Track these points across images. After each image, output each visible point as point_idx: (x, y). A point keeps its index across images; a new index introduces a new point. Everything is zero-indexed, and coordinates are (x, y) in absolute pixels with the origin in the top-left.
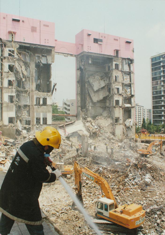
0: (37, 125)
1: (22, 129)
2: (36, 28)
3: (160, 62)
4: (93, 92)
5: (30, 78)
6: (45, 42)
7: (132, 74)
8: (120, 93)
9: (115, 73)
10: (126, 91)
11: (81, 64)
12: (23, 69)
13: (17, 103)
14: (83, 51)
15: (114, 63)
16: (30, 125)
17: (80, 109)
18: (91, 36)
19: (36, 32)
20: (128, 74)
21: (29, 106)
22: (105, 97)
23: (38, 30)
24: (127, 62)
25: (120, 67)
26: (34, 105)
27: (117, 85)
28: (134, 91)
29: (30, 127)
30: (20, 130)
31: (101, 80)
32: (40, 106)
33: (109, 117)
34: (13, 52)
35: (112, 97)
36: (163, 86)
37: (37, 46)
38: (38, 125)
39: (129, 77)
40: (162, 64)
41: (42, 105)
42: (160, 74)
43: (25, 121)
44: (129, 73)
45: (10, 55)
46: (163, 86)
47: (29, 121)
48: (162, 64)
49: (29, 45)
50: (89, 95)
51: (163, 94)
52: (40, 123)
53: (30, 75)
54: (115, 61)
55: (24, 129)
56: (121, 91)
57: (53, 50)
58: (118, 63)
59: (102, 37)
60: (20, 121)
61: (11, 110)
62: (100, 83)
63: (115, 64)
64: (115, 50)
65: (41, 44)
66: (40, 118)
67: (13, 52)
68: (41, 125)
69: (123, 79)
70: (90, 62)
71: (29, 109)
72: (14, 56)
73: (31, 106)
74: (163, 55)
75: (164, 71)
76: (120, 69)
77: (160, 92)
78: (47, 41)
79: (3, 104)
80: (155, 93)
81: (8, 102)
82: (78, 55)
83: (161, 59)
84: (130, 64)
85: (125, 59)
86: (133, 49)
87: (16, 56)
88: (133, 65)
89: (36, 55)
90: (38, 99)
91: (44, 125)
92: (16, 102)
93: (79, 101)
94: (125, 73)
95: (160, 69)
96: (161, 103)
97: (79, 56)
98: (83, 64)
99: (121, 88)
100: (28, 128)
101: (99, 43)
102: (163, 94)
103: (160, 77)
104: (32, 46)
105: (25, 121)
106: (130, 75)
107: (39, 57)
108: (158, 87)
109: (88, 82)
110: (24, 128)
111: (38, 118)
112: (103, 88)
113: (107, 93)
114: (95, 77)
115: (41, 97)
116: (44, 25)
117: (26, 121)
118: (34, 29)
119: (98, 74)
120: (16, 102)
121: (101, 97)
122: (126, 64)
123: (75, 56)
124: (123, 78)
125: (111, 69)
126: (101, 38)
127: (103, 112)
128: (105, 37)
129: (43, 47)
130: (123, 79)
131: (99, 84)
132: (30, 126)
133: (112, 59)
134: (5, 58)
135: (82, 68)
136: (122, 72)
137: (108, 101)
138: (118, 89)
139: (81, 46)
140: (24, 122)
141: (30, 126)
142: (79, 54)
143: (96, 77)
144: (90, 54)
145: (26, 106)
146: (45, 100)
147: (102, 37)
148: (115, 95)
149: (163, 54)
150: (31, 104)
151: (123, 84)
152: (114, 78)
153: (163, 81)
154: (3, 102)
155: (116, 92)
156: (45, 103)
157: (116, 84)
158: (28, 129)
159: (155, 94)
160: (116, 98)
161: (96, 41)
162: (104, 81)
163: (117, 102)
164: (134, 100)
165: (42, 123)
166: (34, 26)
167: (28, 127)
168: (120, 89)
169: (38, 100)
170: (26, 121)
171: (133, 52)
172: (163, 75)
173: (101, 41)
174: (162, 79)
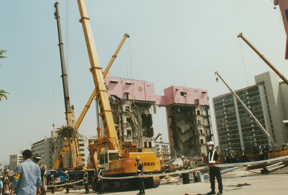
2: (142, 88)
3: (222, 103)
4: (181, 135)
6: (149, 98)
7: (209, 118)
8: (203, 134)
9: (199, 118)
10: (207, 132)
11: (172, 112)
14: (174, 103)
15: (196, 110)
17: (174, 148)
18: (178, 90)
19: (142, 91)
20: (206, 118)
22: (190, 138)
23: (143, 90)
24: (205, 108)
25: (201, 113)
27: (200, 127)
28: (212, 131)
31: (186, 124)
33: (196, 154)
34: (129, 108)
35: (198, 137)
36: (227, 123)
39: (207, 120)
40: (224, 104)
42: (223, 112)
44: (207, 117)
45: (126, 110)
46: (227, 123)
48: (224, 104)
49: (138, 102)
50: (179, 137)
51: (228, 130)
54: (197, 108)
56: (204, 132)
57: (154, 104)
58: (199, 110)
59: (186, 90)
62: (185, 126)
63: (197, 111)
64: (195, 100)
65: (147, 100)
67: (129, 108)
69: (204, 122)
70: (179, 110)
72: (129, 111)
74: (225, 96)
75: (226, 110)
76: (201, 115)
77: (226, 129)
78: (150, 98)
80: (220, 130)
82: (168, 106)
83: (223, 100)
84: (207, 109)
85: (203, 106)
86: (208, 97)
87: (131, 111)
88: (209, 110)
89: (142, 108)
90: (145, 143)
93: (172, 142)
94: (204, 118)
95: (223, 109)
96: (227, 139)
97: (169, 106)
98: (173, 112)
99: (203, 129)
101: (185, 95)
102: (228, 130)
103: (224, 115)
104: (141, 102)
106: (208, 118)
107: (143, 110)
108: (223, 125)
109: (178, 127)
112: (188, 130)
113: (192, 134)
114: (181, 122)
116: (147, 86)
118: (140, 90)
119: (183, 119)
121: (188, 138)
122: (204, 110)
123: (166, 106)
124: (204, 121)
125: (193, 115)
126: (185, 92)
127: (189, 150)
128: (188, 90)
129: (148, 102)
130: (204, 122)
131: (185, 128)
133: (194, 107)
134: (123, 113)
135: (173, 115)
136: (202, 116)
137: (193, 141)
138: (201, 130)
139: (171, 98)
142: (170, 105)
143: (182, 122)
144: (179, 105)
147: (186, 90)
148: (200, 136)
149: (224, 96)
151: (204, 126)
152: (198, 122)
153: (227, 119)
155: (200, 134)
156: (150, 146)
157: (200, 126)
159: (220, 131)
160: (201, 138)
161: (182, 94)
162: (189, 124)
163: (202, 140)
164: (213, 138)
166: (141, 87)
168: (203, 131)
169: (145, 143)
171: (208, 99)
172: (226, 114)
173: (186, 94)
174: (226, 117)
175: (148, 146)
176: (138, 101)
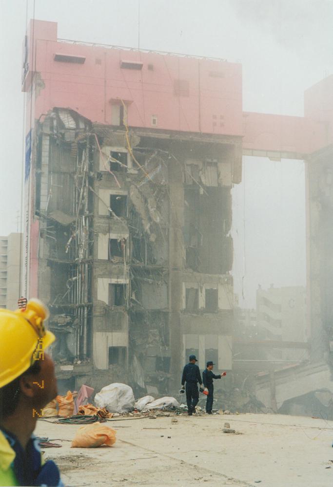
1: (146, 383)
5: (168, 229)
12: (150, 207)
13: (133, 306)
29: (168, 378)
30: (139, 386)
37: (191, 137)
53: (169, 221)
60: (141, 358)
61: (116, 327)
73: (170, 315)
79: (94, 308)
81: (107, 304)
92: (132, 304)
100: (162, 379)
110: (150, 380)
111: (191, 349)
115: (201, 288)
117: (158, 359)
120: (129, 305)
141: (169, 376)
145: (157, 313)
146: (212, 297)
150: (170, 309)
158: (161, 382)
167: (161, 378)
170: (158, 359)
175: (202, 304)
176: (165, 131)
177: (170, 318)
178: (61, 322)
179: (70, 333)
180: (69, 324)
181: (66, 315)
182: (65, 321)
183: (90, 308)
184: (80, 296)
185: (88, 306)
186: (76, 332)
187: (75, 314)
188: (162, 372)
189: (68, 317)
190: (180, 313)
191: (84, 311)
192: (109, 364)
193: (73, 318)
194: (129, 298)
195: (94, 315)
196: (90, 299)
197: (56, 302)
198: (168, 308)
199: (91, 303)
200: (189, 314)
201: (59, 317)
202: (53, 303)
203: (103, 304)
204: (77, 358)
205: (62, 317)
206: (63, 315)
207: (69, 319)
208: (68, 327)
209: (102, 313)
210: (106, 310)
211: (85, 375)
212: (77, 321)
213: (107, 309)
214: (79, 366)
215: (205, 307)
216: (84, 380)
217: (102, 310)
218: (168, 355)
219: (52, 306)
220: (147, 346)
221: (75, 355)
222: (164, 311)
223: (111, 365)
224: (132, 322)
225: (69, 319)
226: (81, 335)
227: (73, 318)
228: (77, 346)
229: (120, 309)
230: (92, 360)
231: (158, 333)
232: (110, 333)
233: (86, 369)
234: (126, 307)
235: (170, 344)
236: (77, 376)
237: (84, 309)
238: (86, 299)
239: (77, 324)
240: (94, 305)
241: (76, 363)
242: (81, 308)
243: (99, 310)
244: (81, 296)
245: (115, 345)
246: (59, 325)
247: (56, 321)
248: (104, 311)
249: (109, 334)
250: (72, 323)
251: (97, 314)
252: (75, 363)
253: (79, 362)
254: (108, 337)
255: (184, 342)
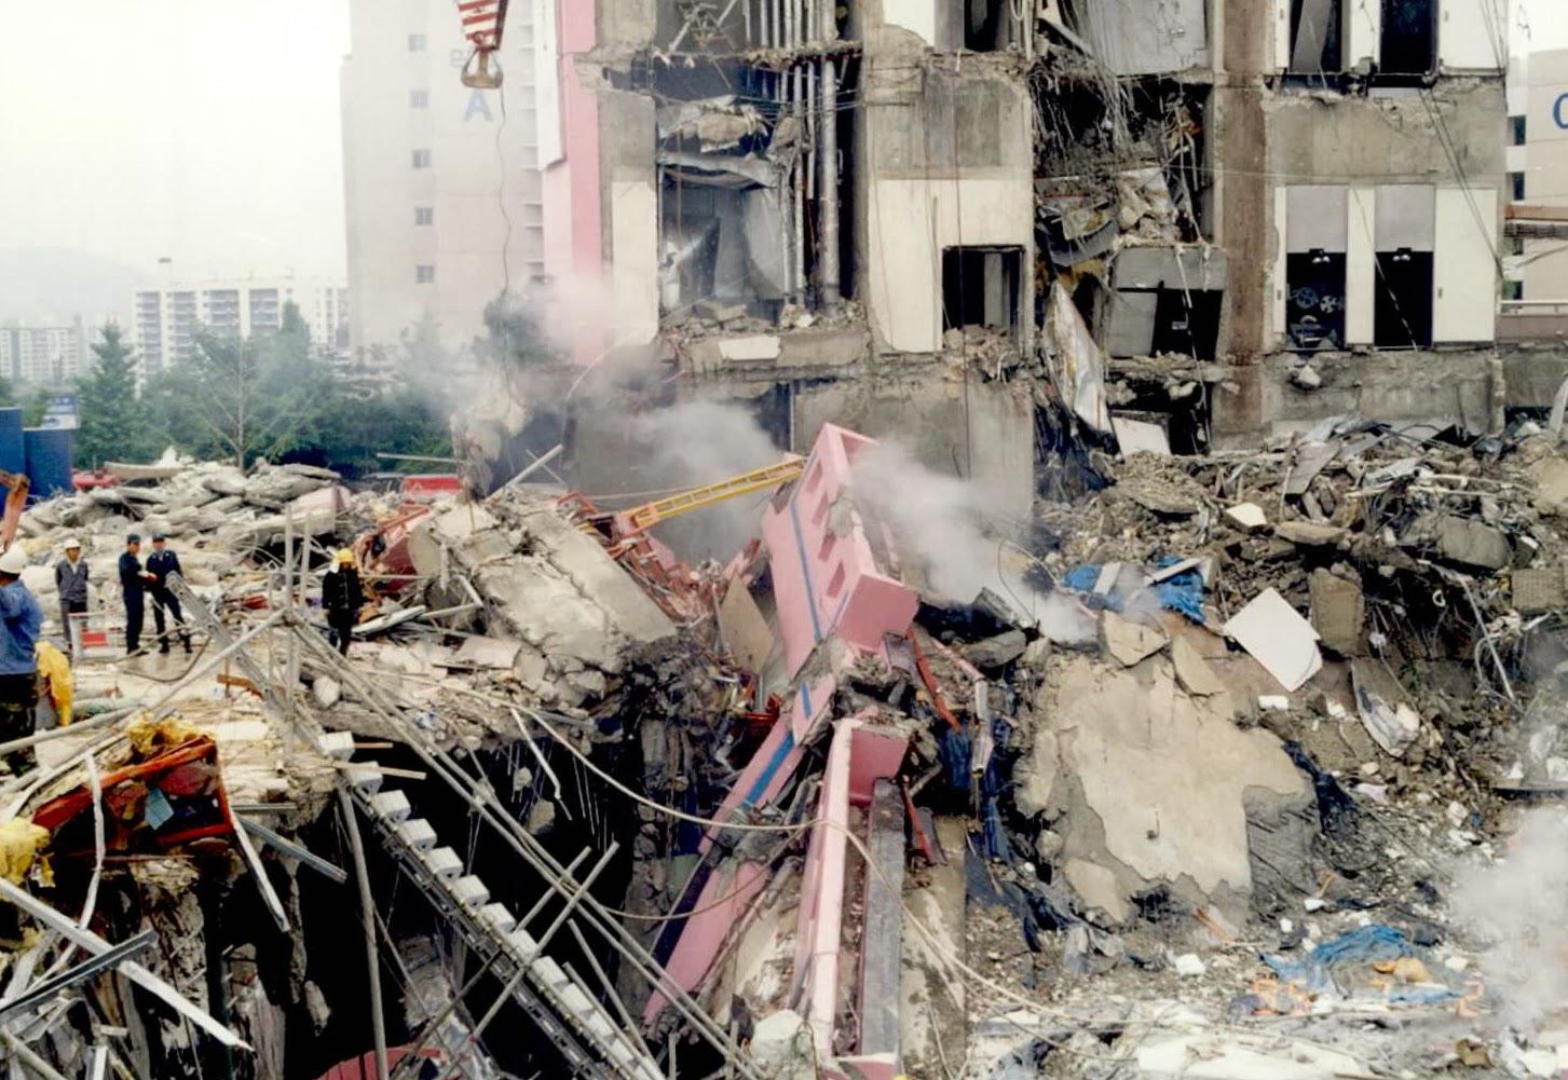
0: (1294, 359)
1: (1114, 409)
13: (1051, 57)
16: (1208, 354)
21: (1201, 92)
26: (1260, 82)
29: (1210, 386)
30: (1082, 424)
32: (1344, 91)
38: (1307, 352)
41: (1379, 78)
43: (1152, 299)
47: (1208, 302)
52: (1334, 323)
55: (1130, 405)
60: (1084, 301)
61: (982, 155)
66: (1339, 260)
68: (1350, 349)
71: (1200, 139)
73: (1218, 99)
79: (865, 66)
81: (931, 42)
91: (1391, 357)
92: (1046, 45)
100: (1187, 390)
105: (1149, 303)
110: (1131, 395)
111: (1315, 253)
117: (1168, 300)
120: (1034, 46)
132: (1212, 372)
140: (1133, 318)
141: (1212, 372)
145: (1152, 95)
150: (1218, 68)
154: (869, 37)
158: (1182, 400)
165: (1360, 323)
167: (1183, 383)
170: (1168, 300)
177: (1218, 116)
178: (711, 134)
179: (758, 186)
180: (753, 144)
181: (737, 102)
182: (730, 131)
183: (850, 67)
184: (788, 13)
185: (841, 55)
186: (786, 180)
187: (781, 97)
188: (1182, 357)
189: (744, 108)
190: (1264, 88)
191: (818, 84)
192: (945, 329)
193: (770, 113)
194: (1035, 10)
195: (867, 98)
196: (844, 25)
197: (689, 44)
198: (1209, 68)
199: (851, 43)
200: (1304, 92)
201: (705, 110)
202: (673, 47)
203: (910, 44)
204: (793, 301)
205: (716, 110)
206: (724, 102)
207: (750, 119)
208: (751, 155)
209: (905, 88)
210: (925, 73)
211: (834, 379)
212: (786, 128)
213: (932, 71)
214: (803, 338)
215: (1377, 59)
216: (828, 397)
217: (906, 74)
218: (1209, 281)
219: (666, 60)
220: (1117, 243)
221: (787, 289)
222: (1192, 80)
223: (954, 333)
224: (1049, 128)
225: (750, 119)
226: (810, 195)
227: (770, 113)
228: (792, 245)
229: (992, 67)
230: (864, 313)
231: (1162, 185)
232: (948, 185)
233: (838, 351)
234: (1020, 57)
235: (1218, 233)
236: (796, 382)
237: (818, 72)
238: (829, 23)
239: (791, 144)
240: (867, 51)
241: (792, 327)
242: (805, 71)
243: (889, 75)
244: (805, 11)
245: (970, 239)
246: (704, 149)
247: (688, 131)
248: (919, 78)
249: (943, 189)
250: (767, 141)
251: (885, 93)
252: (784, 322)
253: (805, 320)
254: (935, 200)
255: (1280, 222)
